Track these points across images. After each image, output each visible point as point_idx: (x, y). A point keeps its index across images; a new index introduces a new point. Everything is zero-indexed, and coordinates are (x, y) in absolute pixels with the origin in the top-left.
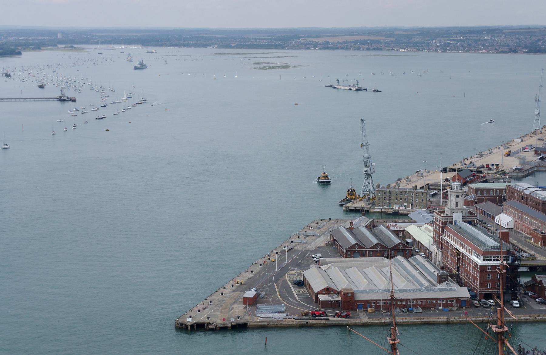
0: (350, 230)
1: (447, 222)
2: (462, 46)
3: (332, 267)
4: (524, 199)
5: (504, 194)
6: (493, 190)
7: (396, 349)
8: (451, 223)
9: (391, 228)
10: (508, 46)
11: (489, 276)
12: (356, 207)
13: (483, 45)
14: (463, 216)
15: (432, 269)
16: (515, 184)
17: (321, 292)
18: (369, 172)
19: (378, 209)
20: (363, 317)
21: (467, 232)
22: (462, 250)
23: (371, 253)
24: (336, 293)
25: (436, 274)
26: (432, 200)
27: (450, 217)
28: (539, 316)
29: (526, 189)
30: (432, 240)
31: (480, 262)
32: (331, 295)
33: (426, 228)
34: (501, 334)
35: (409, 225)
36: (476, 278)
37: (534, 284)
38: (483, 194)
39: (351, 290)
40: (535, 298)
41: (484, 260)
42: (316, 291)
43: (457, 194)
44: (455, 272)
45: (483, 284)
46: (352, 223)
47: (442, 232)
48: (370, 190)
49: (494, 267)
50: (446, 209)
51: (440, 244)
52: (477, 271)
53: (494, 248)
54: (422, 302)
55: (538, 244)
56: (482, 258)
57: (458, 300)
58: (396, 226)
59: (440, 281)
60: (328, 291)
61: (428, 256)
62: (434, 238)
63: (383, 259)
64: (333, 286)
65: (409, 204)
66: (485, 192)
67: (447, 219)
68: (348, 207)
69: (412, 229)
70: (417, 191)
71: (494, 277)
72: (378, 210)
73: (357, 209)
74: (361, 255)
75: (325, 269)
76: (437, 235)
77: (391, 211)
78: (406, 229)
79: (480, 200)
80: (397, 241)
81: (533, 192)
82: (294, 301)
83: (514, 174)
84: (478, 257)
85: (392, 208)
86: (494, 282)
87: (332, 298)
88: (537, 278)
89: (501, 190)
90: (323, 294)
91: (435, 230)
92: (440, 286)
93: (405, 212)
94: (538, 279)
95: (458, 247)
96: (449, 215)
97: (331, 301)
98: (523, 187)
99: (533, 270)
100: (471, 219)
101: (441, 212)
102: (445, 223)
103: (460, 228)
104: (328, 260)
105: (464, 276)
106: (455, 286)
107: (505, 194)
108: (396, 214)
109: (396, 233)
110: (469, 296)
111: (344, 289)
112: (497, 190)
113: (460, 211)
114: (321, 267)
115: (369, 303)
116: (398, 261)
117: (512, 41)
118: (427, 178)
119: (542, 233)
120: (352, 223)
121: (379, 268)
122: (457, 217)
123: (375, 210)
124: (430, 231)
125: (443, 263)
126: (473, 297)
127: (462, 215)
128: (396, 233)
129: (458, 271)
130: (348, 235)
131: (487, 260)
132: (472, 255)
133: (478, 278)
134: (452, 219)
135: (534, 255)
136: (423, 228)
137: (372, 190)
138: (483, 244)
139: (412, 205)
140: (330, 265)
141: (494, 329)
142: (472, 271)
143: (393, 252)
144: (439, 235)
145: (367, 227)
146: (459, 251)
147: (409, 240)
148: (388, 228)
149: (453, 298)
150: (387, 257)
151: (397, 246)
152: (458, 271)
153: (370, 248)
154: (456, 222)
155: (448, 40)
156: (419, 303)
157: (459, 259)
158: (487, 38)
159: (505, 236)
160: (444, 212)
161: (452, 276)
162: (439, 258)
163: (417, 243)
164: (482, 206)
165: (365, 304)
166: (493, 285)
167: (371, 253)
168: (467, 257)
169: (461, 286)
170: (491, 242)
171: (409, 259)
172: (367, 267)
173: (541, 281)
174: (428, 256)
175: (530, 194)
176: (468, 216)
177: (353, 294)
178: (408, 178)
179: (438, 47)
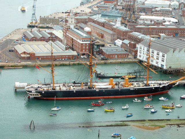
0: (31, 32)
1: (68, 29)
4: (94, 22)
7: (53, 72)
15: (63, 46)
16: (91, 17)
17: (22, 54)
20: (39, 63)
21: (76, 32)
22: (74, 38)
23: (40, 40)
24: (28, 54)
25: (65, 47)
26: (61, 23)
30: (62, 36)
31: (81, 42)
33: (60, 32)
34: (91, 65)
36: (79, 48)
37: (99, 50)
40: (99, 54)
42: (20, 53)
44: (71, 46)
45: (82, 50)
46: (31, 30)
49: (86, 44)
50: (68, 24)
51: (66, 36)
52: (80, 45)
53: (86, 37)
56: (81, 41)
57: (73, 56)
59: (66, 49)
60: (24, 53)
61: (61, 41)
64: (26, 51)
65: (52, 24)
69: (55, 32)
71: (86, 48)
72: (41, 26)
74: (36, 41)
76: (64, 33)
79: (78, 23)
80: (49, 36)
89: (86, 19)
91: (63, 31)
92: (66, 51)
93: (51, 27)
94: (101, 49)
95: (73, 37)
96: (69, 26)
99: (98, 46)
100: (76, 27)
101: (66, 25)
102: (67, 29)
104: (24, 42)
107: (87, 20)
109: (49, 33)
110: (77, 54)
118: (58, 15)
119: (101, 33)
120: (31, 30)
121: (44, 45)
122: (72, 27)
123: (40, 26)
124: (61, 33)
125: (67, 44)
126: (78, 55)
128: (49, 33)
129: (73, 46)
130: (30, 34)
131: (83, 41)
138: (83, 36)
141: (89, 64)
142: (78, 45)
143: (48, 40)
145: (38, 31)
147: (53, 36)
148: (45, 31)
151: (49, 38)
152: (73, 46)
153: (39, 38)
157: (73, 42)
159: (89, 33)
161: (70, 48)
162: (65, 42)
163: (56, 37)
164: (79, 25)
165: (38, 58)
166: (85, 51)
167: (40, 40)
169: (74, 51)
170: (85, 35)
174: (61, 41)
178: (51, 15)
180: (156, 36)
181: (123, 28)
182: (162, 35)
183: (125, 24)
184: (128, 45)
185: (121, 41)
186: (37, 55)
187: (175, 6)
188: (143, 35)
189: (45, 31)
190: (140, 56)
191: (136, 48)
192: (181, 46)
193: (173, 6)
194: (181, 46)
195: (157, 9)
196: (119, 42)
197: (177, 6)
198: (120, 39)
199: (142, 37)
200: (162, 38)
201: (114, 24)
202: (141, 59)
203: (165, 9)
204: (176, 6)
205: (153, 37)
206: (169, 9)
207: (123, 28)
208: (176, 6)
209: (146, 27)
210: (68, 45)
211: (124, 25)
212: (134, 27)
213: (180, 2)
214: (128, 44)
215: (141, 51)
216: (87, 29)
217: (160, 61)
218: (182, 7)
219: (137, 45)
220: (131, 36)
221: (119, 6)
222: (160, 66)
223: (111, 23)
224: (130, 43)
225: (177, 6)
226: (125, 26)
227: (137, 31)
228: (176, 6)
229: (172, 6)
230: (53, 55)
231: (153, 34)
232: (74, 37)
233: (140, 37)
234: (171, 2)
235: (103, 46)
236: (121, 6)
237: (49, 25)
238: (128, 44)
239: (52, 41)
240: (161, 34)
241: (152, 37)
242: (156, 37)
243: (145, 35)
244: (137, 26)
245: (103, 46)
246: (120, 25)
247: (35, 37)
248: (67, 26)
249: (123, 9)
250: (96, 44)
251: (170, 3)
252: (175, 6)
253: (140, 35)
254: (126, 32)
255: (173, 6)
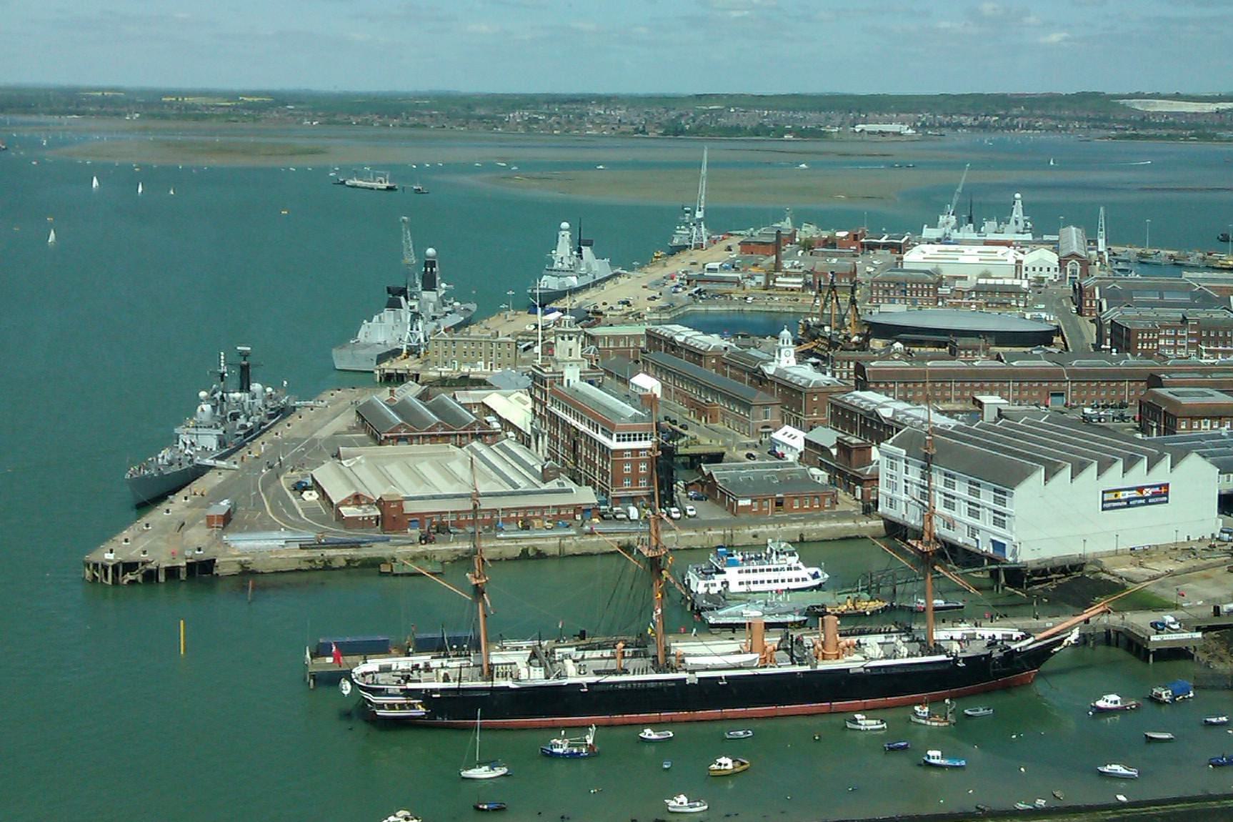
0: (389, 403)
2: (558, 123)
3: (363, 461)
5: (642, 346)
6: (624, 336)
8: (562, 384)
9: (459, 400)
10: (632, 124)
11: (627, 467)
12: (396, 370)
13: (592, 123)
14: (580, 372)
18: (416, 309)
19: (433, 374)
24: (370, 503)
27: (559, 373)
28: (710, 530)
29: (679, 334)
32: (363, 507)
33: (518, 399)
35: (488, 395)
36: (604, 472)
38: (608, 345)
39: (398, 495)
41: (618, 440)
43: (571, 335)
47: (546, 399)
48: (419, 340)
53: (635, 418)
54: (517, 514)
55: (701, 420)
57: (577, 508)
58: (467, 396)
60: (357, 499)
62: (534, 411)
63: (448, 447)
64: (363, 492)
65: (486, 363)
66: (611, 343)
67: (555, 378)
68: (384, 369)
69: (494, 400)
70: (499, 339)
73: (399, 372)
75: (350, 465)
77: (456, 375)
78: (485, 401)
81: (690, 337)
82: (297, 520)
83: (656, 317)
84: (610, 436)
85: (459, 370)
86: (635, 477)
87: (365, 511)
88: (704, 469)
89: (636, 338)
90: (349, 506)
93: (481, 376)
97: (363, 517)
98: (674, 331)
99: (694, 461)
101: (545, 367)
103: (577, 391)
105: (583, 468)
106: (570, 485)
108: (466, 382)
110: (596, 501)
111: (385, 495)
112: (630, 336)
113: (575, 364)
114: (343, 462)
115: (428, 518)
116: (473, 450)
117: (638, 116)
120: (392, 391)
122: (572, 375)
124: (525, 403)
127: (578, 370)
129: (576, 464)
131: (624, 440)
132: (597, 433)
133: (609, 470)
134: (563, 377)
135: (695, 438)
136: (512, 398)
137: (422, 341)
139: (491, 365)
140: (358, 458)
144: (542, 406)
145: (419, 397)
146: (577, 430)
149: (569, 506)
150: (456, 445)
154: (568, 381)
155: (535, 114)
156: (513, 515)
158: (597, 111)
160: (549, 366)
162: (544, 443)
168: (591, 438)
170: (629, 410)
171: (493, 447)
172: (423, 461)
173: (711, 474)
175: (686, 340)
176: (588, 372)
177: (400, 503)
179: (518, 123)
180: (958, 407)
181: (807, 374)
182: (991, 400)
183: (817, 356)
184: (834, 452)
185: (801, 435)
186: (410, 508)
187: (1041, 269)
188: (901, 406)
189: (454, 397)
190: (892, 502)
191: (871, 463)
192: (1083, 454)
193: (1034, 269)
194: (1083, 454)
195: (958, 284)
196: (791, 439)
197: (1052, 270)
198: (797, 424)
199: (895, 412)
200: (989, 415)
201: (765, 356)
202: (896, 514)
203: (999, 282)
204: (1048, 269)
205: (950, 414)
206: (1017, 282)
207: (807, 374)
208: (1045, 269)
209: (916, 367)
210: (556, 459)
211: (814, 360)
212: (860, 369)
213: (1063, 254)
214: (833, 447)
215: (891, 476)
216: (647, 382)
217: (985, 522)
218: (1074, 272)
219: (874, 449)
220: (844, 410)
221: (787, 275)
222: (987, 548)
223: (753, 352)
224: (840, 445)
225: (1052, 270)
226: (814, 364)
227: (872, 386)
228: (1048, 269)
229: (1026, 269)
230: (486, 504)
231: (948, 400)
232: (582, 421)
233: (886, 413)
234: (1023, 253)
235: (717, 458)
236: (797, 275)
237: (473, 370)
238: (833, 447)
239: (484, 442)
240: (985, 399)
241: (942, 413)
242: (961, 412)
243: (907, 406)
244: (873, 364)
245: (717, 458)
246: (793, 362)
247: (406, 427)
248: (550, 370)
249: (807, 285)
250: (681, 450)
251: (1020, 257)
252: (1041, 269)
253: (886, 405)
254: (823, 392)
255: (1034, 269)
